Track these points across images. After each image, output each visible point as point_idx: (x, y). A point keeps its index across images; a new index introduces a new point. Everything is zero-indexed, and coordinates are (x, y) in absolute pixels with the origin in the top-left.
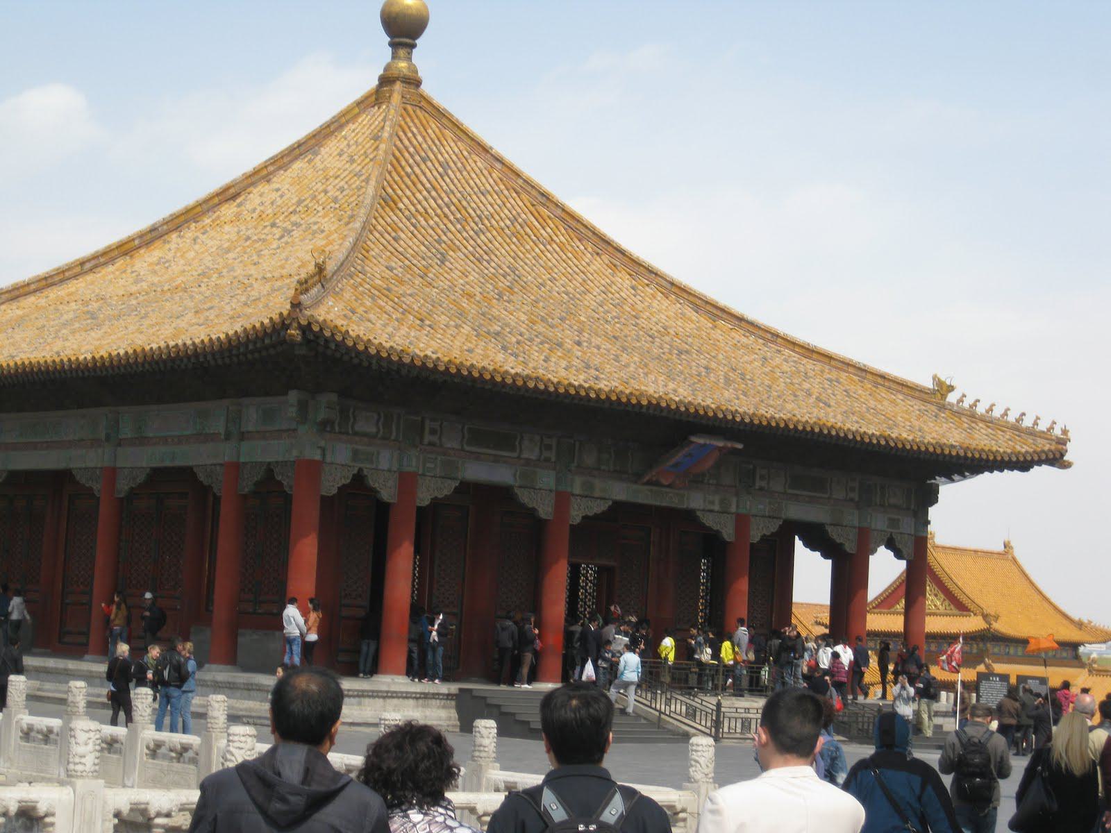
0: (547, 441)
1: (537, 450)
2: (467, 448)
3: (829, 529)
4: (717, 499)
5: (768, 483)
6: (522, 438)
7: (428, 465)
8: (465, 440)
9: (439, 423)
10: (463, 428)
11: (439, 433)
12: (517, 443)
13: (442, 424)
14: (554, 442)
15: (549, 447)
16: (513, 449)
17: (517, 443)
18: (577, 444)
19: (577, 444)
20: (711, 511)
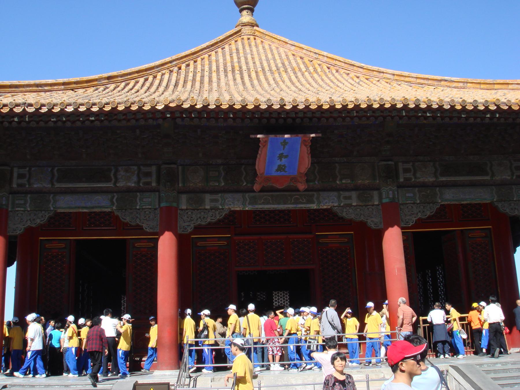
0: (144, 169)
1: (135, 178)
2: (57, 185)
3: (500, 205)
4: (354, 194)
5: (414, 174)
6: (117, 171)
7: (17, 202)
8: (55, 178)
9: (28, 169)
10: (52, 171)
11: (28, 176)
12: (112, 175)
13: (30, 169)
14: (154, 169)
15: (148, 174)
16: (108, 180)
17: (112, 175)
18: (180, 168)
19: (180, 168)
20: (350, 206)
